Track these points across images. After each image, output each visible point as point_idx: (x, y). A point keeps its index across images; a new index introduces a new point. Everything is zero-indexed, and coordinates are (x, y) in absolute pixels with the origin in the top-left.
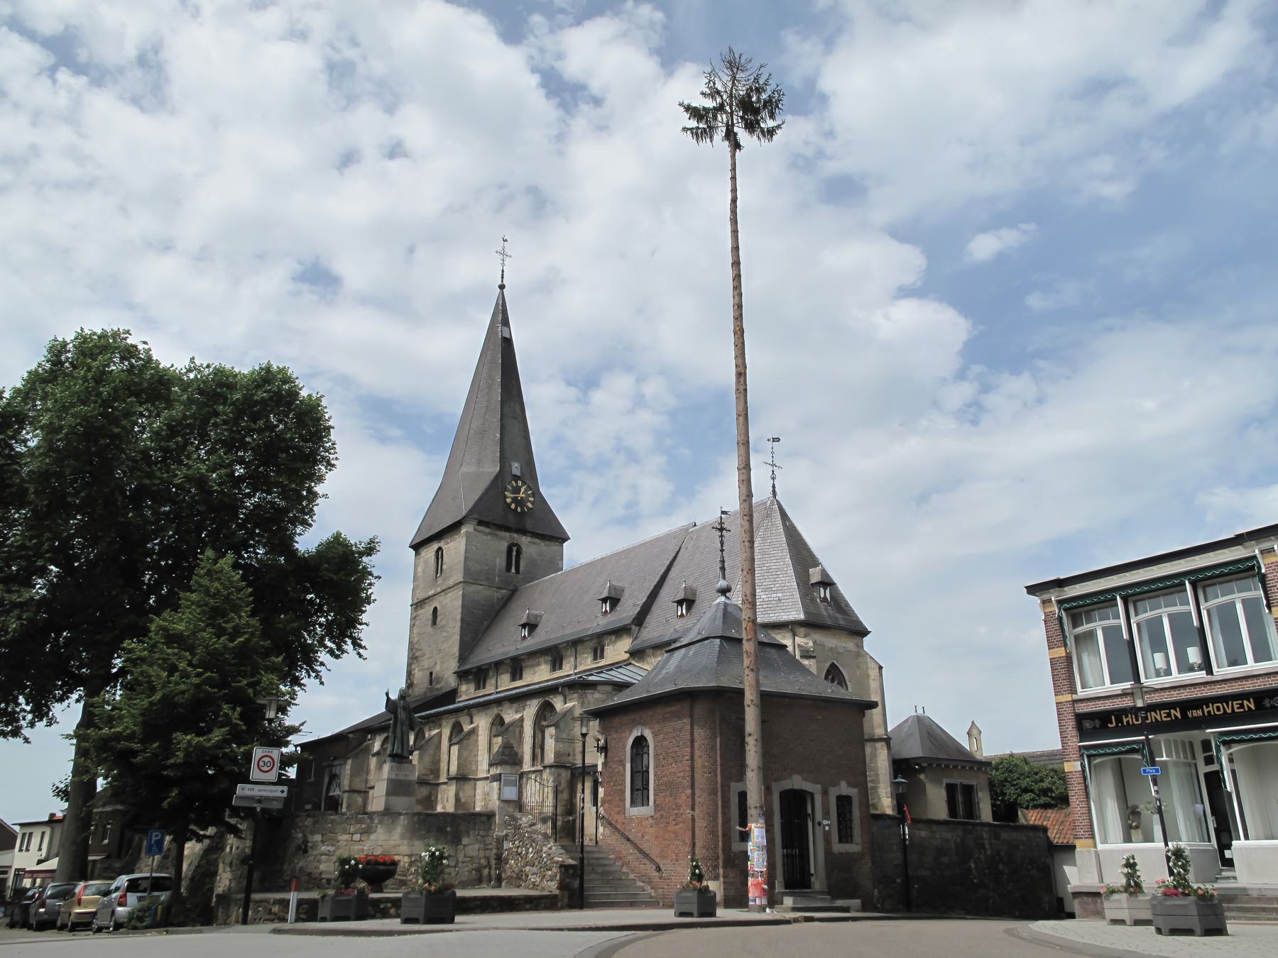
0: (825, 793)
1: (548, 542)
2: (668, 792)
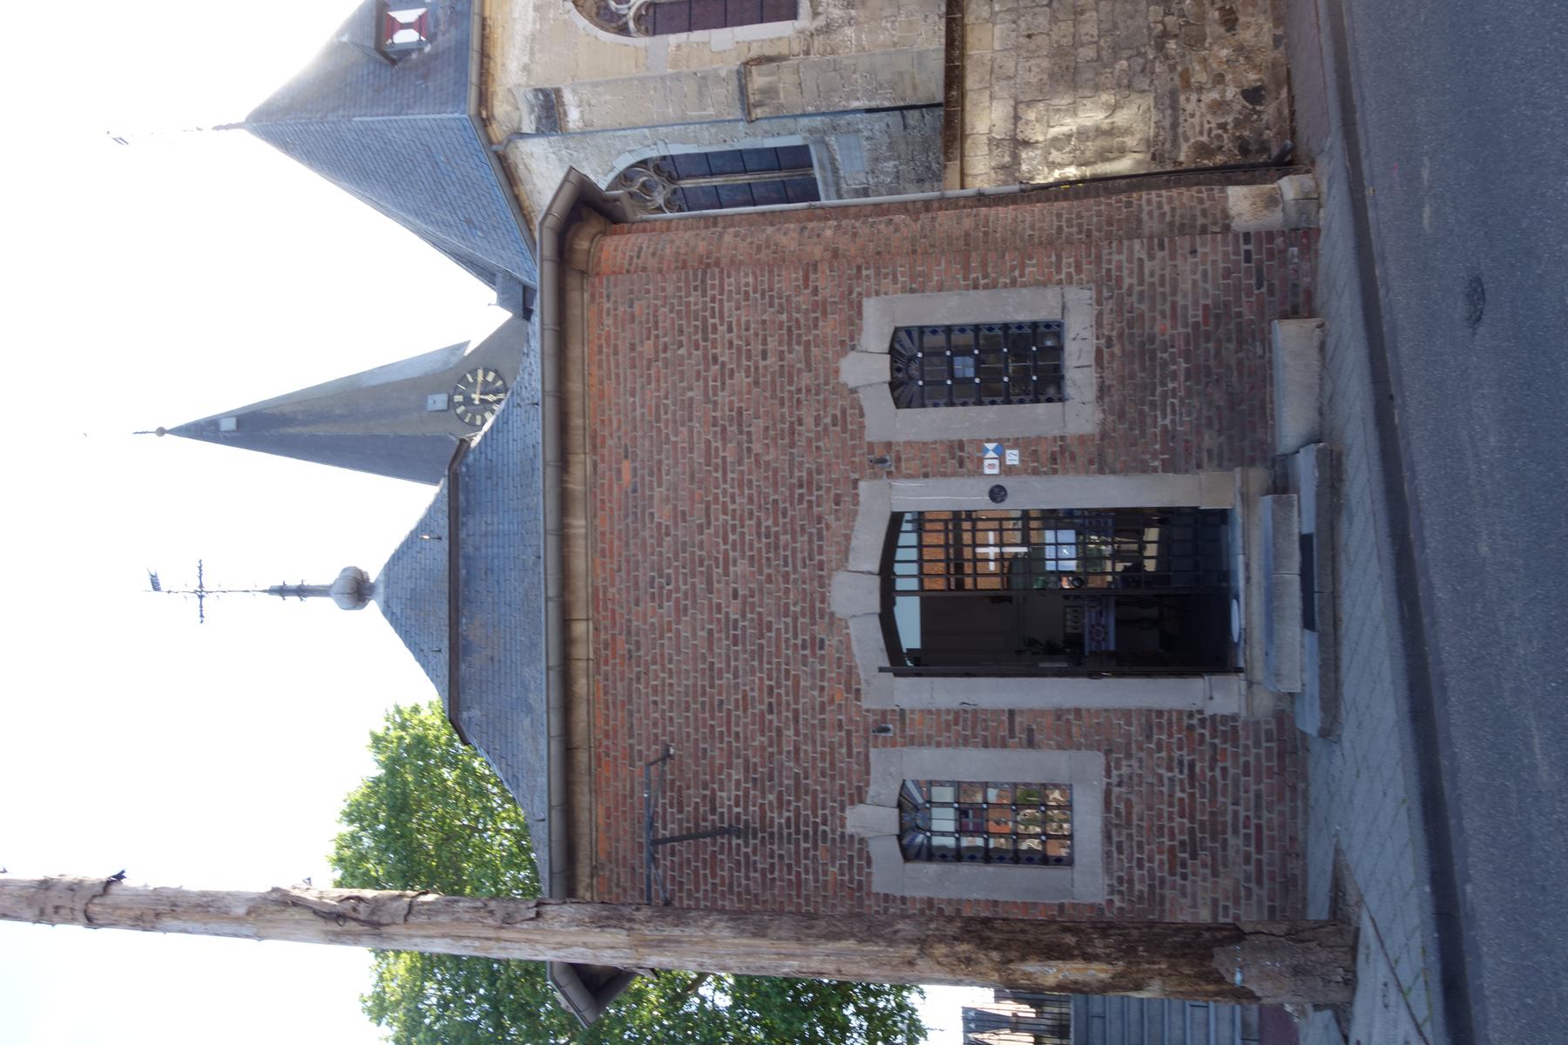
0: (885, 461)
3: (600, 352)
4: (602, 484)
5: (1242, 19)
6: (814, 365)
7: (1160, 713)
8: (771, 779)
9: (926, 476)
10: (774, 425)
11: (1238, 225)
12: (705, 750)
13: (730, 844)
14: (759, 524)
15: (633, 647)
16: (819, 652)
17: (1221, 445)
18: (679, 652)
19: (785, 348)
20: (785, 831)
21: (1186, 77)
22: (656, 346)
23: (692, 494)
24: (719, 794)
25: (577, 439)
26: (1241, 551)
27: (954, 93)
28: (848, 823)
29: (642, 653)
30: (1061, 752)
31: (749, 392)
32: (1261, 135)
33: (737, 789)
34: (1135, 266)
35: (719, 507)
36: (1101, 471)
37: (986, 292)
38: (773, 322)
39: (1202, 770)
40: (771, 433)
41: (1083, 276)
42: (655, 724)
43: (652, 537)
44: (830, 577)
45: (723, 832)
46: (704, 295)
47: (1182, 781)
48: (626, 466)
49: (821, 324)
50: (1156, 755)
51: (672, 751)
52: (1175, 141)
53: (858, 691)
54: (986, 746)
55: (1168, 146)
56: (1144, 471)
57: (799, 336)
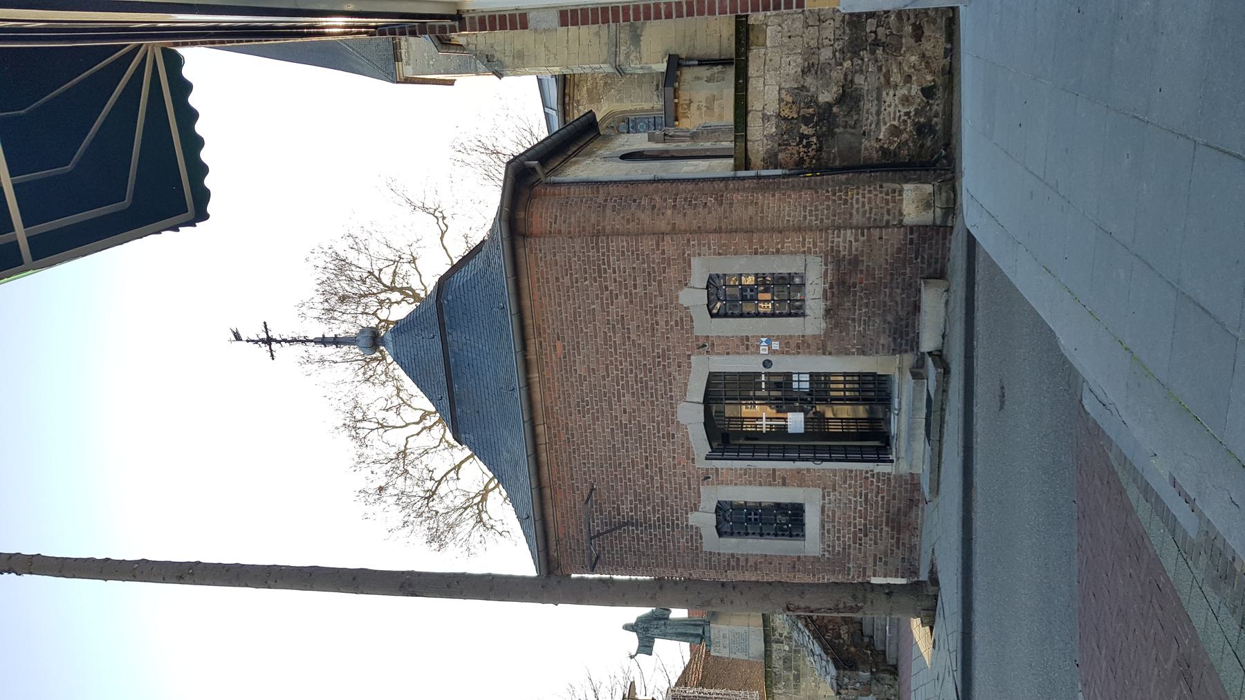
0: (705, 346)
3: (539, 282)
4: (546, 354)
5: (927, 33)
6: (663, 294)
7: (851, 471)
8: (649, 499)
9: (728, 354)
10: (642, 325)
11: (908, 220)
12: (613, 486)
13: (628, 529)
14: (636, 376)
15: (570, 437)
16: (671, 440)
17: (889, 341)
18: (596, 439)
19: (647, 283)
20: (657, 523)
21: (887, 76)
22: (571, 280)
23: (598, 359)
24: (621, 506)
25: (530, 330)
26: (897, 396)
27: (741, 81)
28: (690, 521)
29: (575, 439)
30: (800, 488)
31: (627, 307)
32: (931, 121)
33: (631, 504)
34: (847, 245)
35: (614, 367)
36: (824, 353)
37: (762, 256)
38: (640, 269)
39: (872, 497)
40: (641, 329)
41: (817, 249)
42: (585, 474)
43: (576, 381)
44: (677, 404)
45: (625, 524)
46: (598, 252)
47: (861, 502)
48: (559, 344)
49: (667, 271)
50: (848, 490)
51: (595, 486)
52: (878, 124)
53: (693, 459)
54: (760, 485)
55: (873, 126)
56: (846, 354)
57: (655, 277)
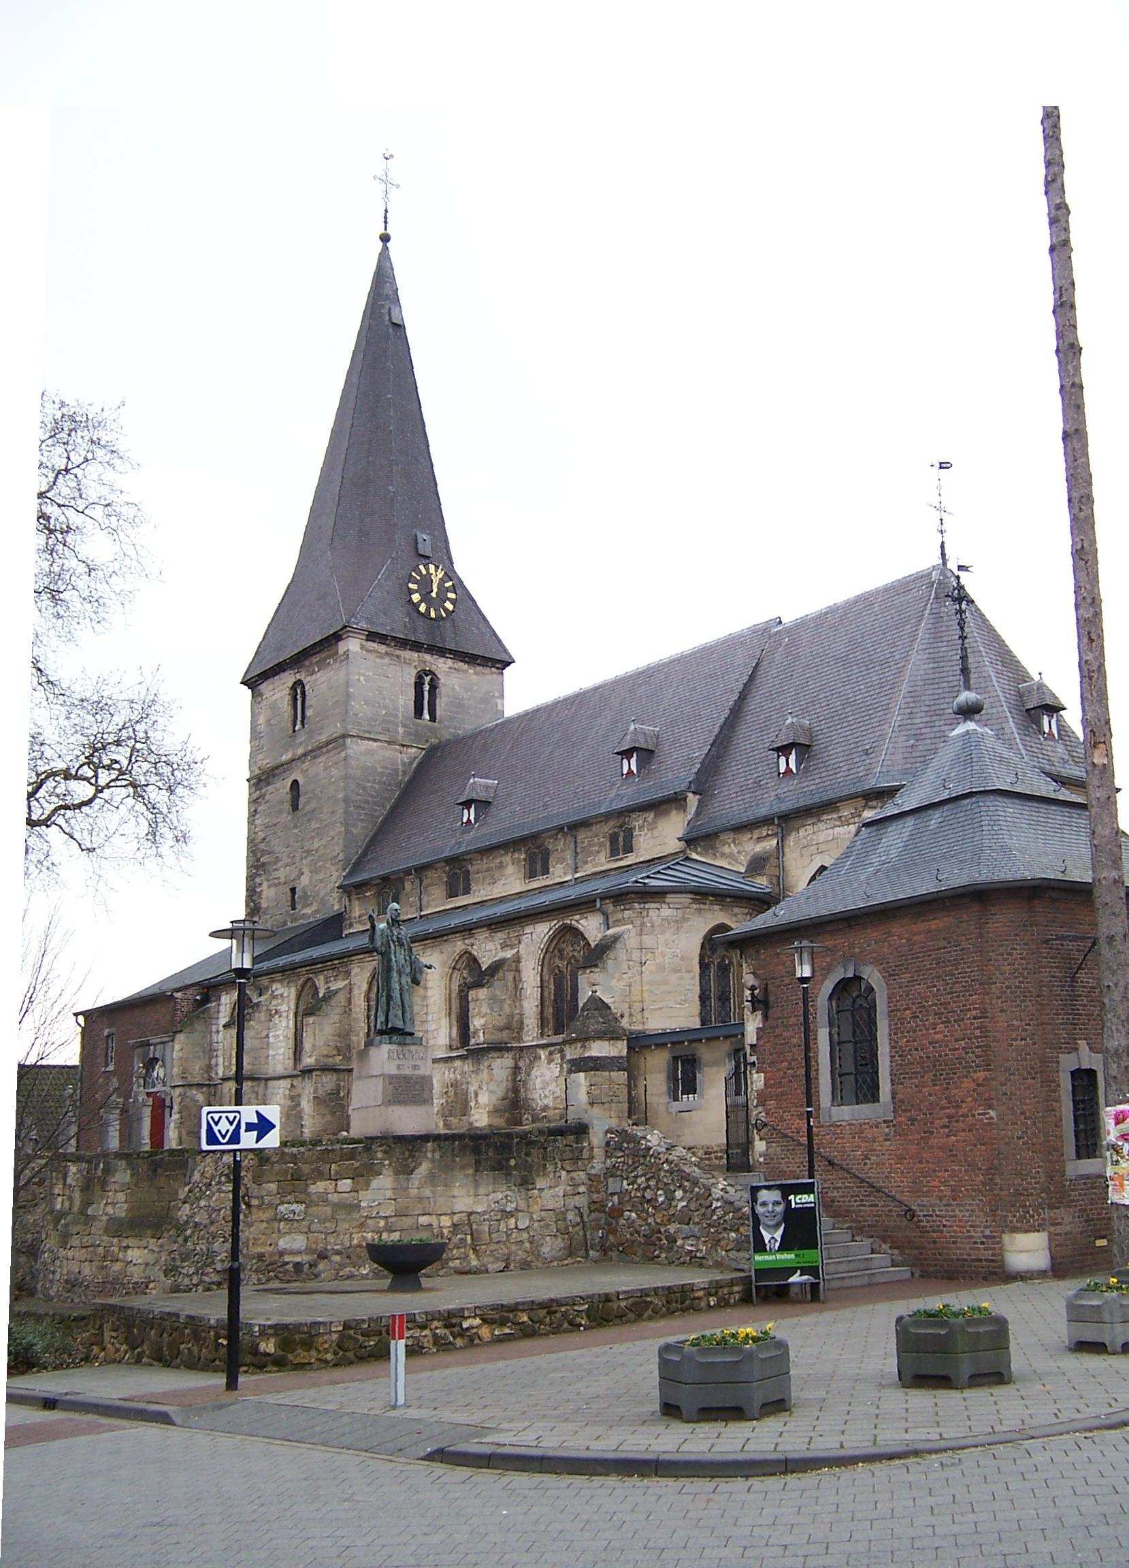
1: (479, 668)
2: (928, 1078)
8: (1092, 1001)
